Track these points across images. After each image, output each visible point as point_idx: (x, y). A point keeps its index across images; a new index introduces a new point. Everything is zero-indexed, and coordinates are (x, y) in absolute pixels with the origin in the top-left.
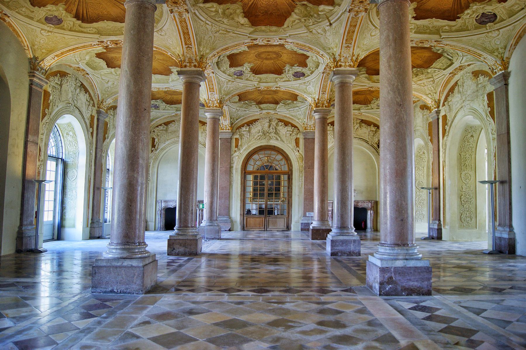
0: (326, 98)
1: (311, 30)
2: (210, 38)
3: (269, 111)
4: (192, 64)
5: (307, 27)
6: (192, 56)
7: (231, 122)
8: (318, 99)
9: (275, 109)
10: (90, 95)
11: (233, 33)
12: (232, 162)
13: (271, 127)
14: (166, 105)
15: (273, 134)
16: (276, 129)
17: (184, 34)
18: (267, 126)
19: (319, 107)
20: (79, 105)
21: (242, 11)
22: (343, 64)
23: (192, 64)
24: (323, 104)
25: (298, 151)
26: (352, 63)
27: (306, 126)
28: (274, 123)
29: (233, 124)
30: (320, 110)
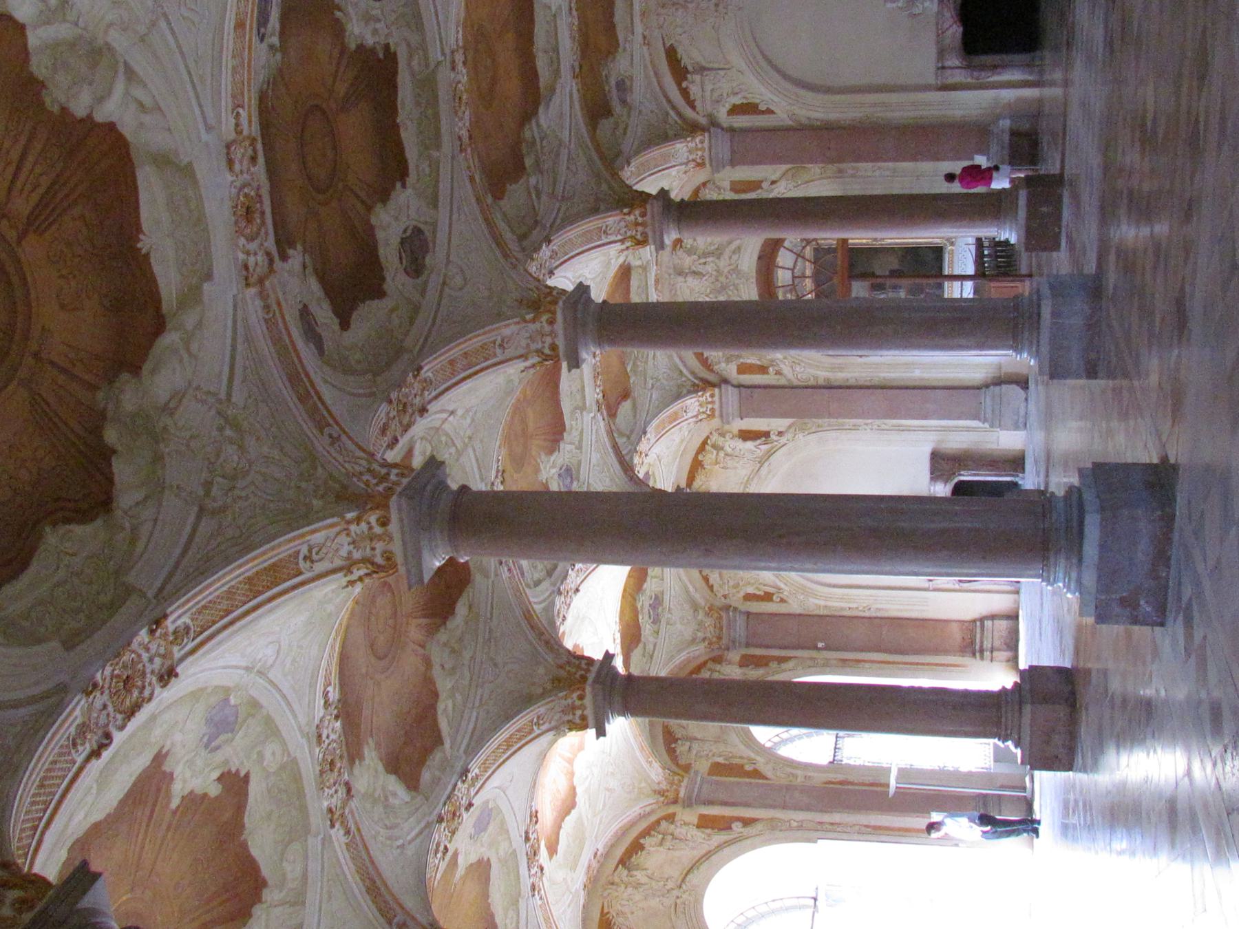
0: (617, 218)
1: (466, 440)
2: (510, 675)
3: (651, 281)
4: (578, 703)
5: (459, 454)
6: (558, 709)
7: (689, 392)
8: (622, 241)
9: (644, 268)
10: (647, 833)
11: (491, 619)
12: (812, 382)
13: (701, 269)
14: (649, 579)
15: (723, 263)
16: (705, 255)
17: (509, 746)
18: (696, 282)
19: (644, 234)
20: (676, 873)
21: (442, 630)
22: (548, 340)
23: (578, 703)
24: (637, 224)
25: (773, 182)
26: (545, 318)
27: (692, 165)
28: (687, 261)
29: (694, 385)
30: (654, 232)
